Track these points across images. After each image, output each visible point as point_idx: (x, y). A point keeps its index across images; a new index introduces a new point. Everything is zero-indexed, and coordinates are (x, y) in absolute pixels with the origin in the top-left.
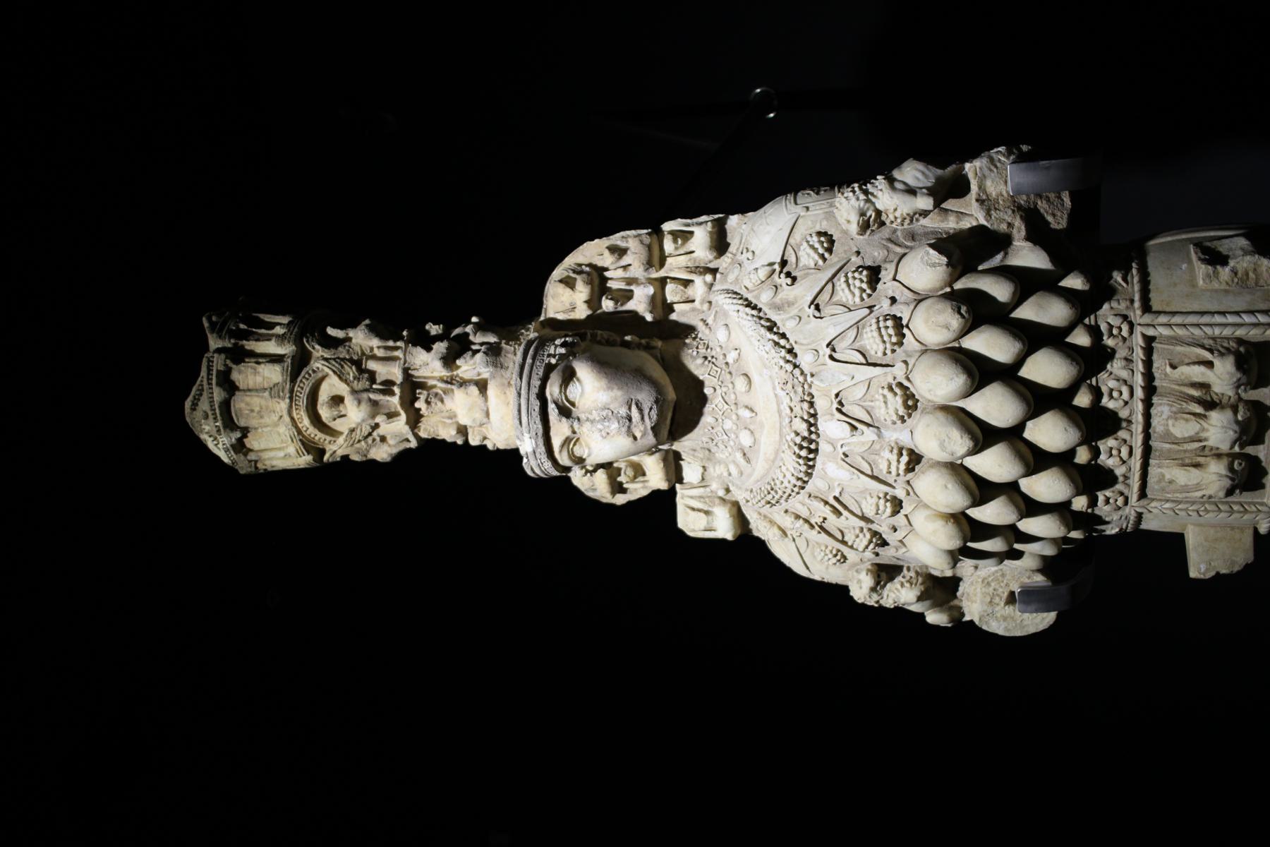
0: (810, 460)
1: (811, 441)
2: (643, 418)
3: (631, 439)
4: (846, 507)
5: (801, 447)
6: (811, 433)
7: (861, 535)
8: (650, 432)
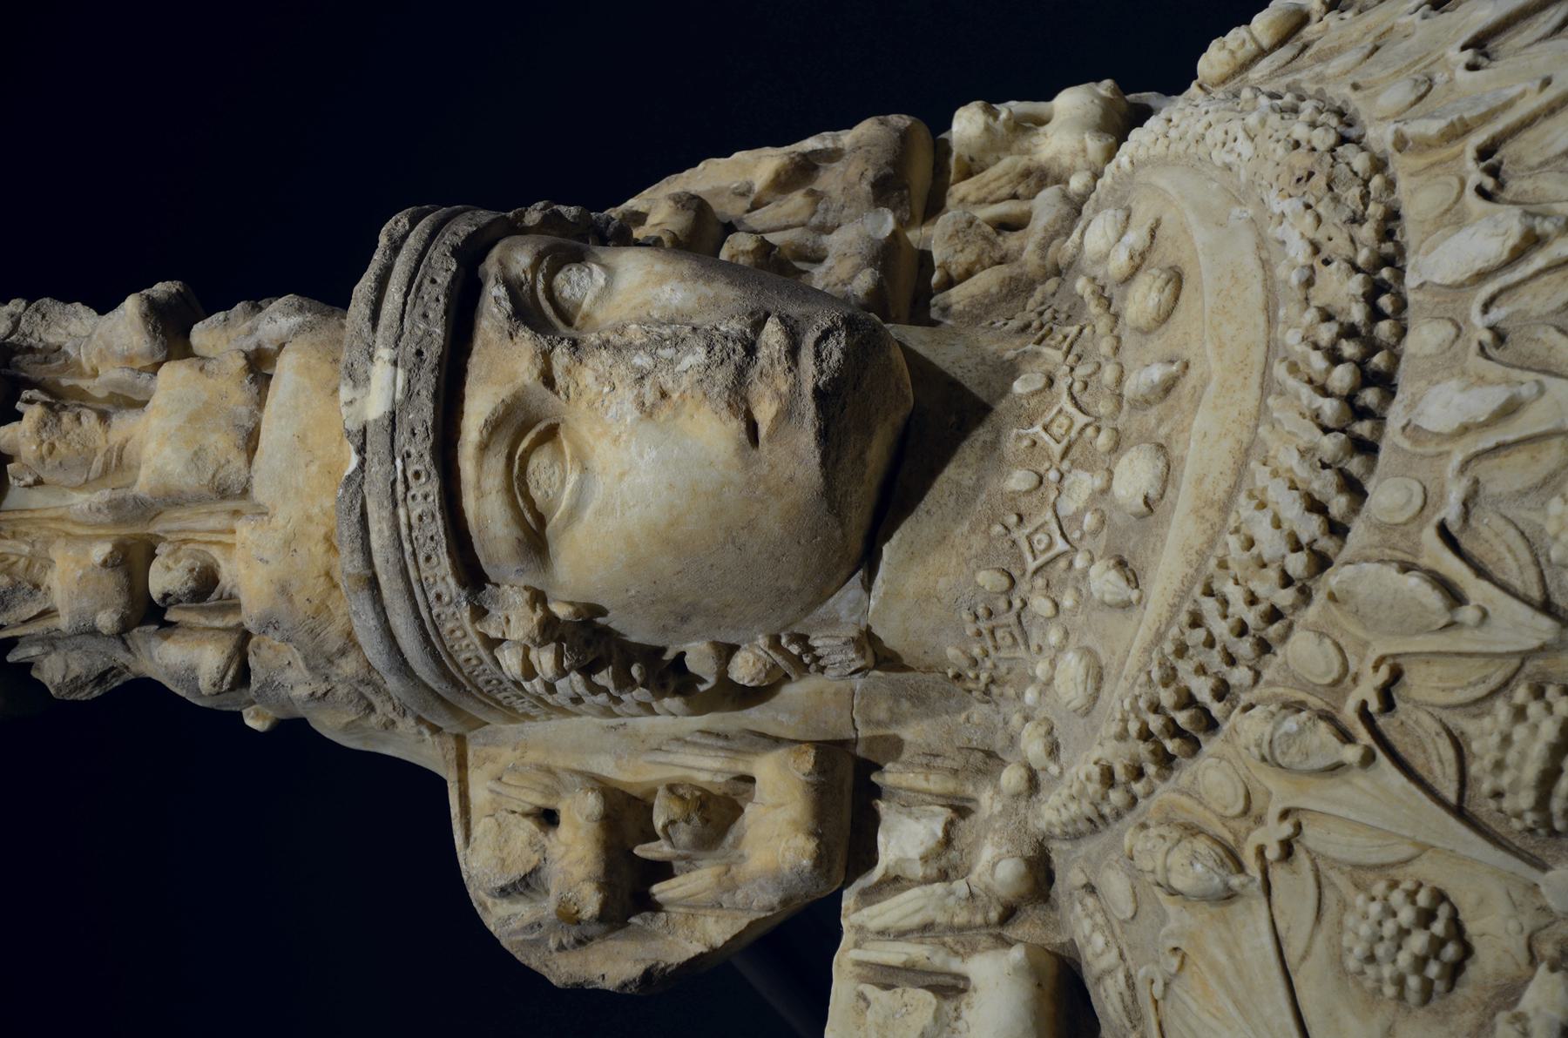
0: (1362, 413)
1: (1372, 347)
2: (793, 352)
3: (737, 426)
4: (1481, 572)
5: (1335, 358)
6: (1376, 315)
7: (1534, 709)
8: (809, 407)
